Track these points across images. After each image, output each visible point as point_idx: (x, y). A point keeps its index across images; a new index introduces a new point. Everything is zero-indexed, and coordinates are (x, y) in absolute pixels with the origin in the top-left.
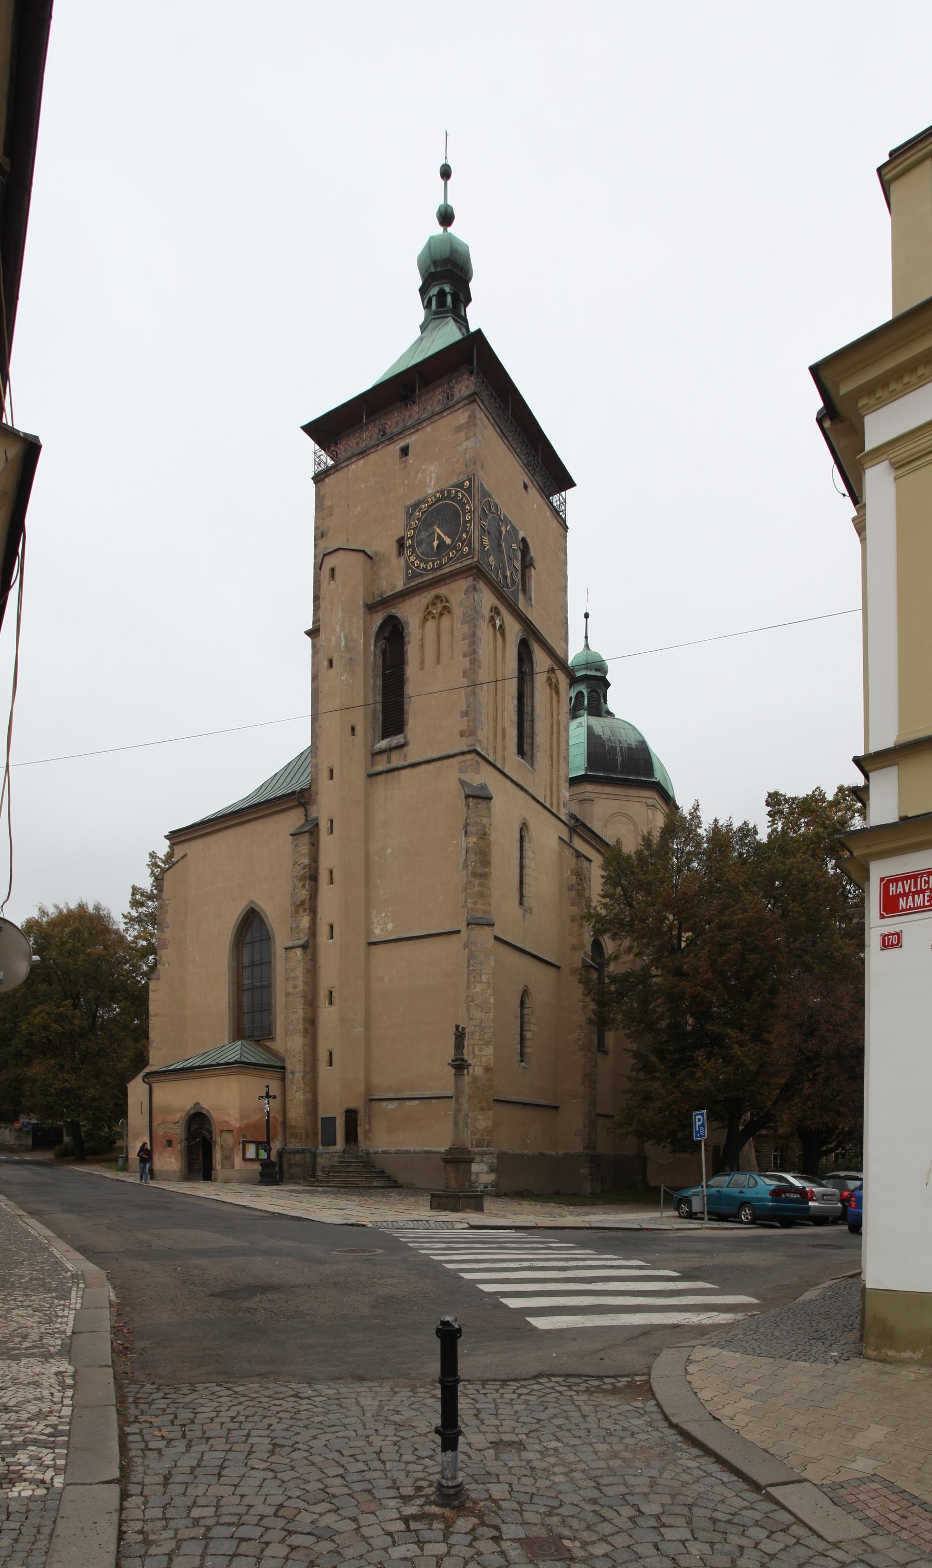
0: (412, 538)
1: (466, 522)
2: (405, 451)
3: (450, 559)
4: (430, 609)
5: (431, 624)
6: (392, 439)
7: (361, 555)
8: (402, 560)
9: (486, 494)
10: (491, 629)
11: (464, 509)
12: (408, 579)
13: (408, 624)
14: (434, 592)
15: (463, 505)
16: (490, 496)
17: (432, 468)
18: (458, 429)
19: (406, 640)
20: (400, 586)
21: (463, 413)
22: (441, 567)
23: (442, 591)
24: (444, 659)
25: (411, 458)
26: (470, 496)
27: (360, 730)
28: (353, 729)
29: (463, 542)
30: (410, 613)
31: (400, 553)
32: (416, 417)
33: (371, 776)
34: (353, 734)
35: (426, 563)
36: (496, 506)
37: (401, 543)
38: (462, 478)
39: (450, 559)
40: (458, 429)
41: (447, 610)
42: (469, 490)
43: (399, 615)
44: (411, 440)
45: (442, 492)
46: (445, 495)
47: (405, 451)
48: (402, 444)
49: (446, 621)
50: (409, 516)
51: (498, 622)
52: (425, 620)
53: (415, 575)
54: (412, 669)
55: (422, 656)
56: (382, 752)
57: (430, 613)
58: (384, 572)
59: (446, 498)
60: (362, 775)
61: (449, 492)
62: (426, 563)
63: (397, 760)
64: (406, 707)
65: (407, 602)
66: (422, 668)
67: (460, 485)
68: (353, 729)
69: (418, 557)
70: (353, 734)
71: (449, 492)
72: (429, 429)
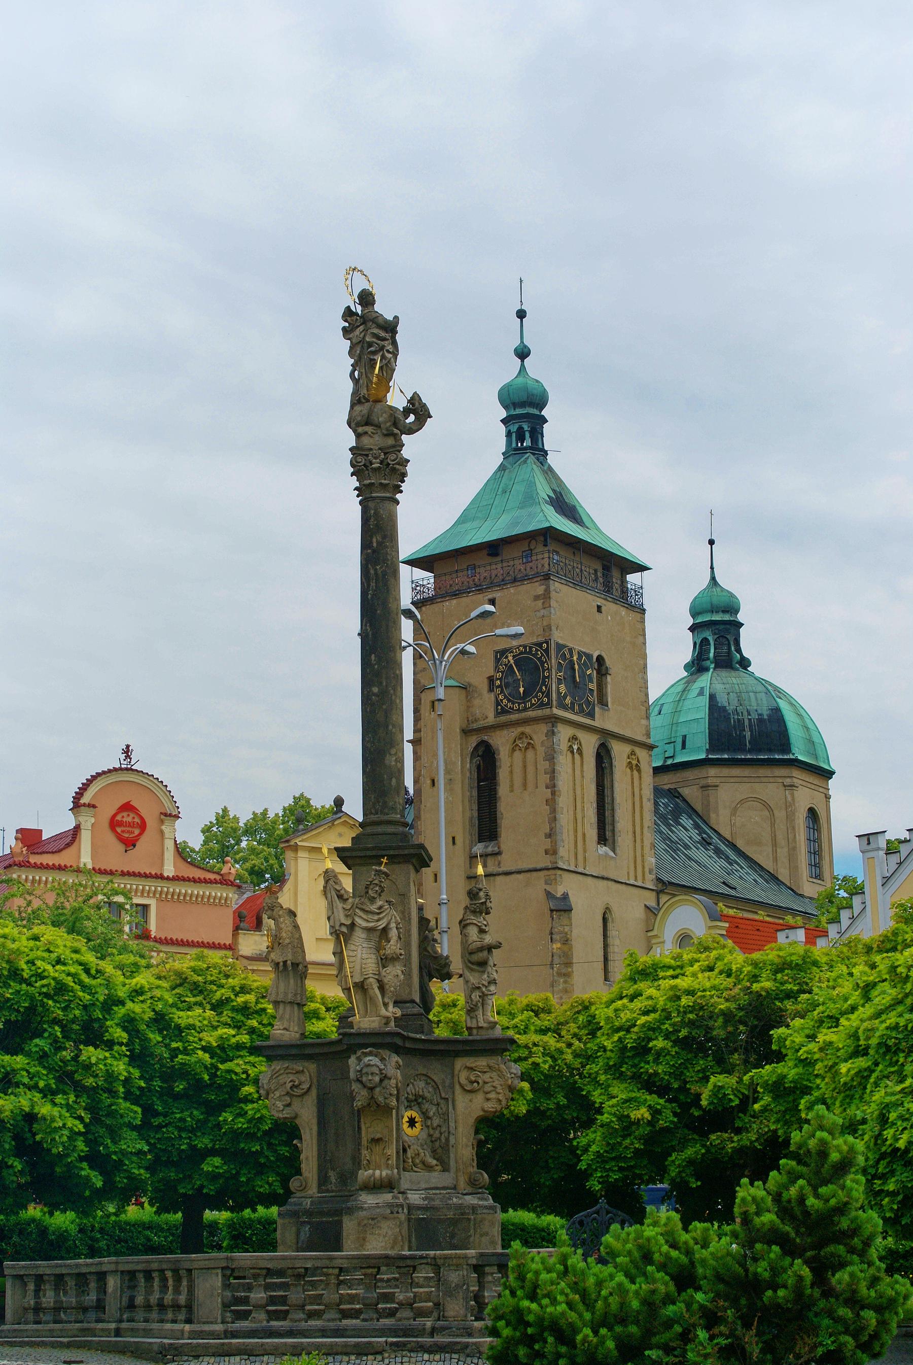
0: (500, 679)
1: (545, 677)
3: (532, 705)
4: (518, 742)
5: (518, 754)
7: (457, 689)
8: (492, 695)
9: (560, 647)
10: (569, 754)
11: (543, 666)
12: (497, 714)
13: (498, 749)
14: (520, 729)
15: (542, 663)
16: (565, 646)
18: (537, 598)
19: (498, 764)
20: (491, 719)
21: (540, 585)
22: (525, 709)
23: (527, 729)
26: (548, 655)
28: (454, 838)
29: (543, 694)
30: (501, 742)
31: (491, 690)
32: (501, 577)
34: (454, 843)
35: (513, 704)
37: (491, 680)
38: (541, 639)
39: (532, 705)
41: (530, 746)
42: (547, 651)
43: (491, 741)
44: (497, 595)
45: (525, 647)
48: (490, 596)
49: (530, 754)
50: (497, 660)
51: (575, 747)
52: (513, 750)
53: (504, 712)
54: (503, 790)
55: (512, 780)
57: (517, 745)
58: (477, 702)
59: (528, 653)
60: (463, 876)
61: (530, 648)
62: (513, 704)
64: (498, 821)
65: (498, 733)
66: (512, 791)
67: (540, 645)
68: (454, 838)
69: (505, 697)
70: (454, 843)
71: (530, 648)
72: (512, 590)
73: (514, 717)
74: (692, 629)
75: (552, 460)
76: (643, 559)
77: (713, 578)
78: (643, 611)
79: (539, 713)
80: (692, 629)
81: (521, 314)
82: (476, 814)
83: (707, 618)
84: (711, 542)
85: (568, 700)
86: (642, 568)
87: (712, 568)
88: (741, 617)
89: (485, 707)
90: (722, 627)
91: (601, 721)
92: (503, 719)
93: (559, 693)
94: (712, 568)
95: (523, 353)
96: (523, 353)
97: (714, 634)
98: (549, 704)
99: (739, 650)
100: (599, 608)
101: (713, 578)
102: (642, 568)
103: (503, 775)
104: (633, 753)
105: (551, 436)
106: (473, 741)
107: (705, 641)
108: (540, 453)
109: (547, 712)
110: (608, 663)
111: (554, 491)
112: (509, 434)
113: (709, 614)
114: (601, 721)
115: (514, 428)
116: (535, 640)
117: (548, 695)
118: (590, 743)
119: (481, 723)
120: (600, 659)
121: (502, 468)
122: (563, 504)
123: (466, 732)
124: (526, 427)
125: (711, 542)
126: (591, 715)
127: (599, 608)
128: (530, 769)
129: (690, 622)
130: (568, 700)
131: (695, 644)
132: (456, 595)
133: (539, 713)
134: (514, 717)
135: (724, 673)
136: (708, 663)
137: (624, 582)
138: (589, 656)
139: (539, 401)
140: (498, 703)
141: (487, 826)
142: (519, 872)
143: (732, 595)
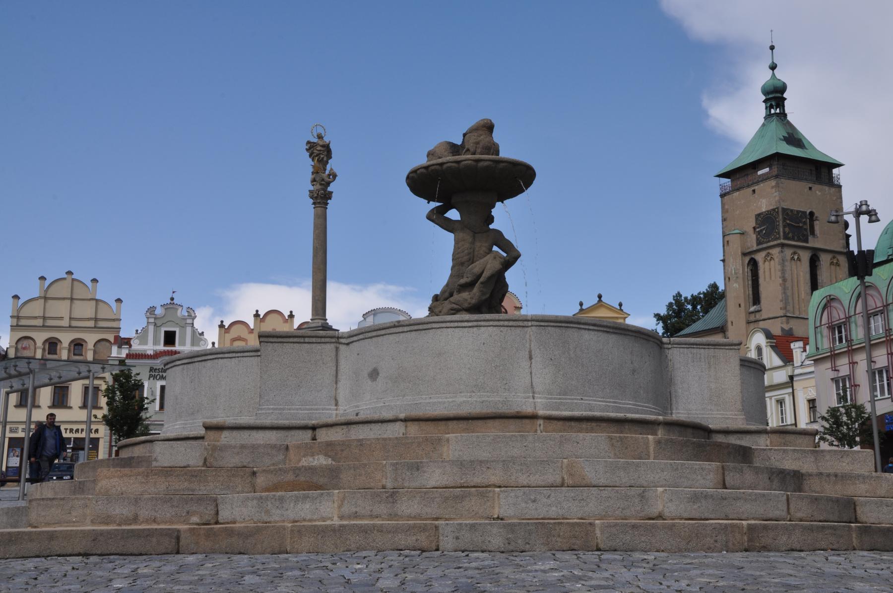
2: (754, 191)
5: (767, 263)
6: (748, 186)
17: (764, 201)
18: (773, 187)
22: (769, 241)
24: (773, 278)
25: (756, 195)
27: (743, 305)
30: (759, 257)
33: (749, 323)
36: (792, 211)
37: (754, 228)
40: (773, 187)
42: (778, 212)
44: (756, 188)
46: (769, 213)
47: (754, 191)
49: (772, 262)
50: (757, 219)
54: (761, 281)
56: (752, 313)
60: (744, 322)
63: (758, 316)
67: (774, 210)
73: (764, 246)
75: (789, 118)
76: (842, 162)
78: (840, 187)
79: (775, 242)
81: (772, 48)
82: (751, 292)
85: (790, 235)
86: (839, 165)
89: (752, 242)
91: (812, 243)
92: (761, 247)
93: (784, 232)
95: (773, 67)
96: (773, 67)
98: (779, 238)
100: (810, 188)
102: (839, 165)
103: (761, 272)
104: (834, 257)
105: (788, 107)
106: (747, 259)
108: (783, 115)
109: (779, 242)
110: (816, 215)
111: (788, 133)
112: (766, 108)
114: (812, 243)
115: (768, 105)
116: (772, 208)
117: (779, 233)
118: (806, 256)
119: (751, 250)
120: (812, 214)
121: (764, 125)
122: (794, 138)
123: (744, 254)
124: (774, 103)
126: (807, 241)
127: (810, 188)
128: (773, 270)
130: (790, 235)
132: (738, 190)
133: (775, 242)
134: (764, 246)
137: (830, 173)
138: (804, 213)
139: (783, 89)
140: (757, 239)
141: (756, 300)
142: (769, 319)
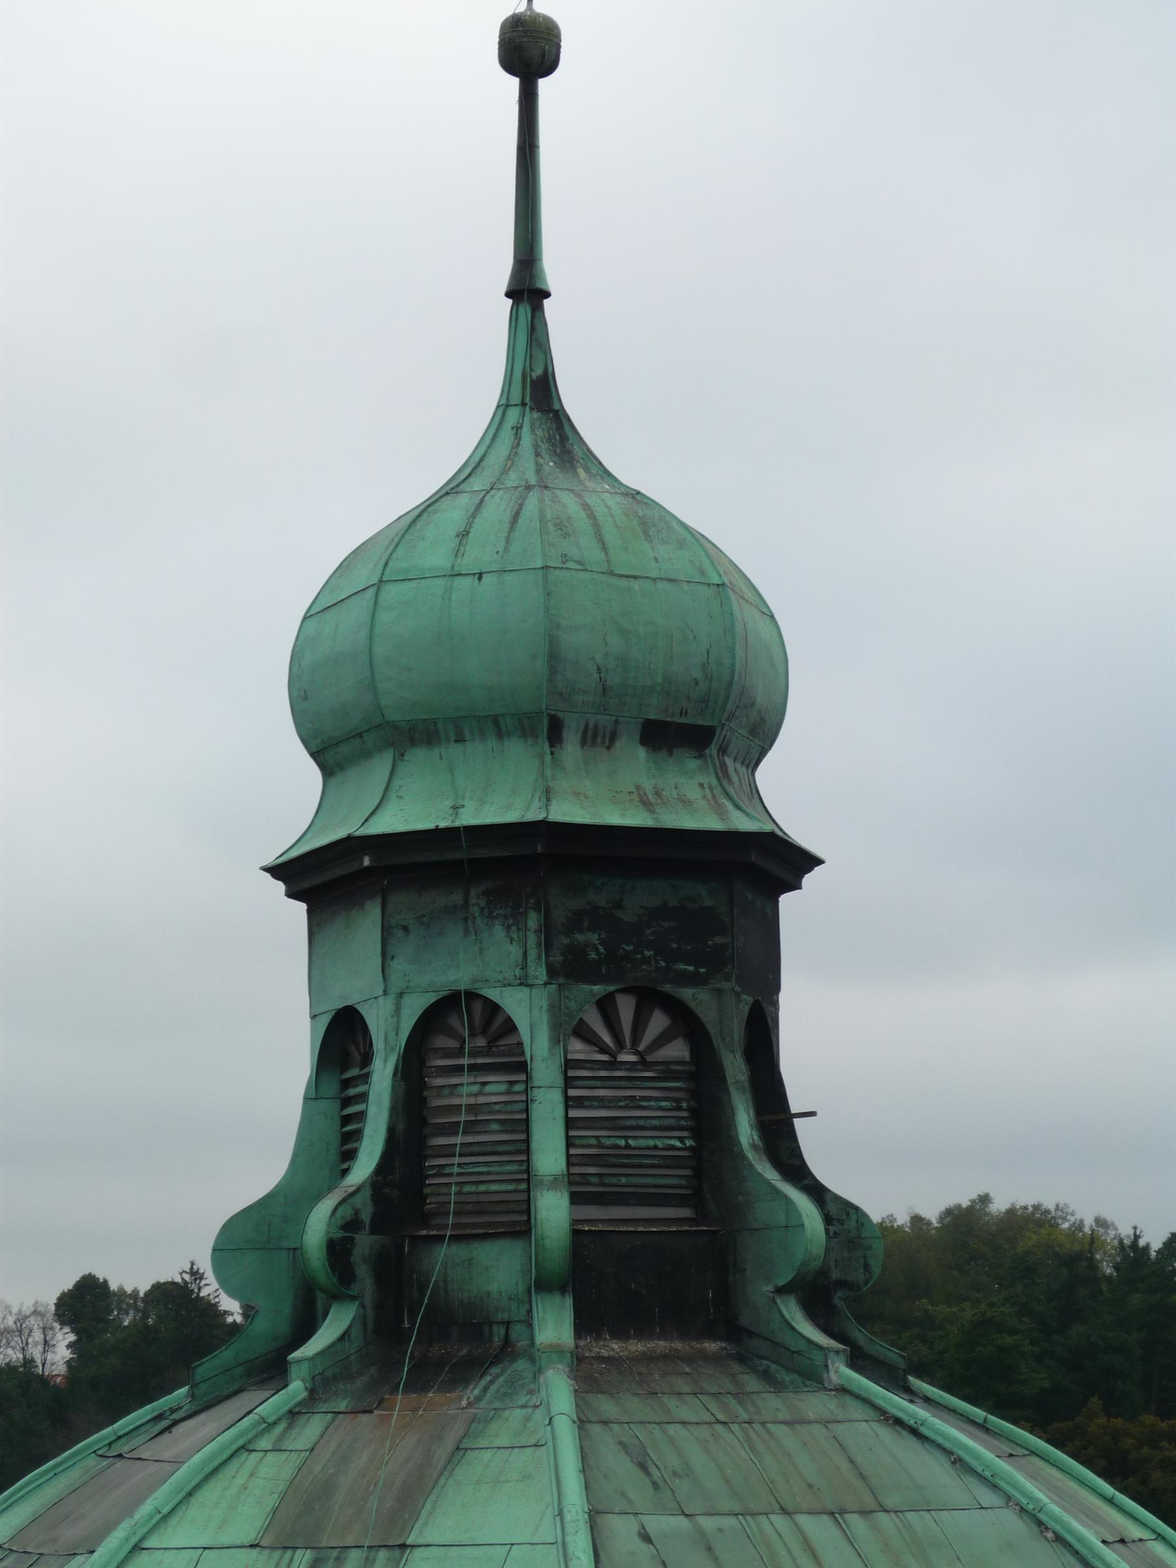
74: (322, 879)
77: (534, 391)
80: (322, 879)
83: (493, 793)
84: (529, 51)
87: (527, 291)
88: (790, 788)
90: (640, 898)
94: (527, 291)
97: (569, 968)
99: (796, 1170)
101: (534, 391)
107: (459, 1023)
113: (519, 759)
125: (529, 51)
129: (291, 800)
131: (342, 1042)
135: (699, 1431)
136: (496, 1270)
143: (723, 589)
